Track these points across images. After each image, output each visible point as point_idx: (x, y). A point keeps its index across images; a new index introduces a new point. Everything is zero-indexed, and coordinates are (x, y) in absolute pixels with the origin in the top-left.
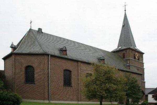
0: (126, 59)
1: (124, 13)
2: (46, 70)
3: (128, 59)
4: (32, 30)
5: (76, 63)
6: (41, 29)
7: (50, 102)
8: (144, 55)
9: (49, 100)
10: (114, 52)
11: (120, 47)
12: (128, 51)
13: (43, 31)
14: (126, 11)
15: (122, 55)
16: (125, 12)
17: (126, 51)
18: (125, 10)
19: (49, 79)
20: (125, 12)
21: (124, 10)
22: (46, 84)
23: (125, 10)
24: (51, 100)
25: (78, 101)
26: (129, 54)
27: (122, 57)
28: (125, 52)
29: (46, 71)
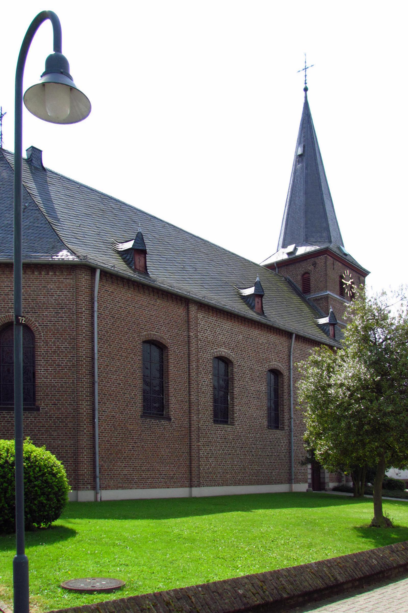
0: (313, 295)
1: (303, 101)
2: (85, 344)
3: (321, 298)
4: (4, 150)
5: (180, 311)
6: (41, 151)
7: (99, 496)
8: (368, 279)
9: (94, 488)
10: (271, 267)
11: (290, 244)
12: (320, 260)
13: (46, 163)
14: (308, 92)
15: (299, 277)
16: (306, 97)
17: (315, 264)
18: (306, 90)
19: (96, 385)
20: (306, 97)
21: (304, 86)
22: (85, 407)
23: (306, 90)
24: (102, 488)
25: (191, 486)
26: (326, 275)
27: (300, 288)
28: (311, 268)
29: (84, 352)
